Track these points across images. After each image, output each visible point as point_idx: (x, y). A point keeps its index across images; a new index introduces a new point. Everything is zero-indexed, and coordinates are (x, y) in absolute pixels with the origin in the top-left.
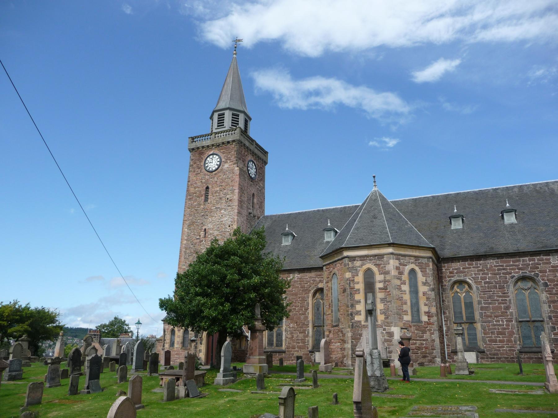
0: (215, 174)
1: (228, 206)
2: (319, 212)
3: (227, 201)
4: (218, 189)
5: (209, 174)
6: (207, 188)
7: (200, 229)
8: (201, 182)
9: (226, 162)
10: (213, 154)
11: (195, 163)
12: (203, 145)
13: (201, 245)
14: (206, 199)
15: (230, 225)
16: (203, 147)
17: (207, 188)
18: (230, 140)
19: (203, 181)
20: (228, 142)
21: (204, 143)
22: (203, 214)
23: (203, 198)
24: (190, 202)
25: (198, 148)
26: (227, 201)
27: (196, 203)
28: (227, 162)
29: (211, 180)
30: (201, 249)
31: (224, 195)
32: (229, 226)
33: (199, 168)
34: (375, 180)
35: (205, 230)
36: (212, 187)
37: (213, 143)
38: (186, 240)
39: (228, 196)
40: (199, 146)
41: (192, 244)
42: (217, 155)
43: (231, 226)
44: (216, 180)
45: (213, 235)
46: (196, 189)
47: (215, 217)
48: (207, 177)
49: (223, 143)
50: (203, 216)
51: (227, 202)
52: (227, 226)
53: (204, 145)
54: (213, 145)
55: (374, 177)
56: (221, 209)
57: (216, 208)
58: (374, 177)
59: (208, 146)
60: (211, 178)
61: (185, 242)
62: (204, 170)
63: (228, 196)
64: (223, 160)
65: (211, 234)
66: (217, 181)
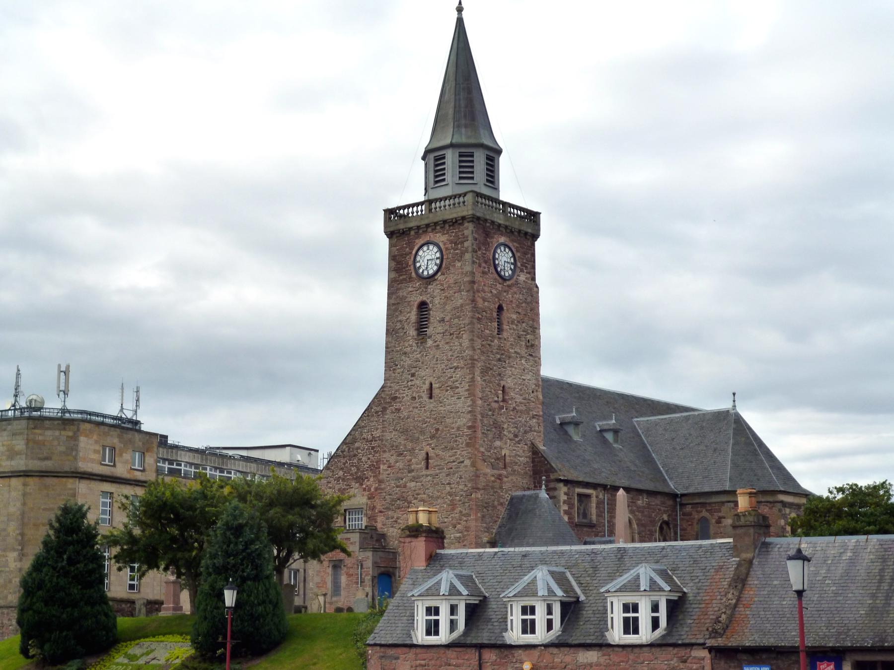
0: (508, 286)
1: (531, 355)
2: (562, 388)
3: (528, 344)
4: (514, 316)
5: (500, 281)
6: (500, 309)
7: (498, 385)
8: (491, 292)
9: (522, 271)
10: (506, 246)
11: (480, 249)
12: (493, 219)
13: (501, 415)
14: (500, 330)
15: (535, 391)
16: (493, 222)
17: (500, 309)
18: (530, 231)
19: (494, 292)
20: (526, 233)
21: (495, 215)
22: (499, 356)
23: (496, 324)
24: (479, 326)
25: (486, 220)
26: (528, 344)
27: (487, 332)
28: (524, 272)
29: (505, 294)
30: (502, 422)
31: (523, 331)
32: (533, 392)
33: (486, 262)
34: (734, 398)
35: (504, 387)
36: (507, 310)
37: (507, 223)
38: (480, 398)
39: (528, 337)
40: (488, 217)
41: (490, 410)
42: (510, 249)
43: (535, 393)
44: (511, 299)
45: (516, 402)
46: (486, 304)
47: (516, 368)
48: (499, 287)
49: (519, 231)
50: (499, 360)
51: (527, 347)
52: (531, 392)
53: (495, 220)
54: (506, 227)
55: (734, 394)
56: (522, 357)
57: (515, 352)
58: (734, 394)
59: (499, 225)
60: (505, 292)
61: (479, 402)
62: (492, 269)
63: (528, 337)
64: (519, 264)
65: (512, 398)
66: (512, 301)
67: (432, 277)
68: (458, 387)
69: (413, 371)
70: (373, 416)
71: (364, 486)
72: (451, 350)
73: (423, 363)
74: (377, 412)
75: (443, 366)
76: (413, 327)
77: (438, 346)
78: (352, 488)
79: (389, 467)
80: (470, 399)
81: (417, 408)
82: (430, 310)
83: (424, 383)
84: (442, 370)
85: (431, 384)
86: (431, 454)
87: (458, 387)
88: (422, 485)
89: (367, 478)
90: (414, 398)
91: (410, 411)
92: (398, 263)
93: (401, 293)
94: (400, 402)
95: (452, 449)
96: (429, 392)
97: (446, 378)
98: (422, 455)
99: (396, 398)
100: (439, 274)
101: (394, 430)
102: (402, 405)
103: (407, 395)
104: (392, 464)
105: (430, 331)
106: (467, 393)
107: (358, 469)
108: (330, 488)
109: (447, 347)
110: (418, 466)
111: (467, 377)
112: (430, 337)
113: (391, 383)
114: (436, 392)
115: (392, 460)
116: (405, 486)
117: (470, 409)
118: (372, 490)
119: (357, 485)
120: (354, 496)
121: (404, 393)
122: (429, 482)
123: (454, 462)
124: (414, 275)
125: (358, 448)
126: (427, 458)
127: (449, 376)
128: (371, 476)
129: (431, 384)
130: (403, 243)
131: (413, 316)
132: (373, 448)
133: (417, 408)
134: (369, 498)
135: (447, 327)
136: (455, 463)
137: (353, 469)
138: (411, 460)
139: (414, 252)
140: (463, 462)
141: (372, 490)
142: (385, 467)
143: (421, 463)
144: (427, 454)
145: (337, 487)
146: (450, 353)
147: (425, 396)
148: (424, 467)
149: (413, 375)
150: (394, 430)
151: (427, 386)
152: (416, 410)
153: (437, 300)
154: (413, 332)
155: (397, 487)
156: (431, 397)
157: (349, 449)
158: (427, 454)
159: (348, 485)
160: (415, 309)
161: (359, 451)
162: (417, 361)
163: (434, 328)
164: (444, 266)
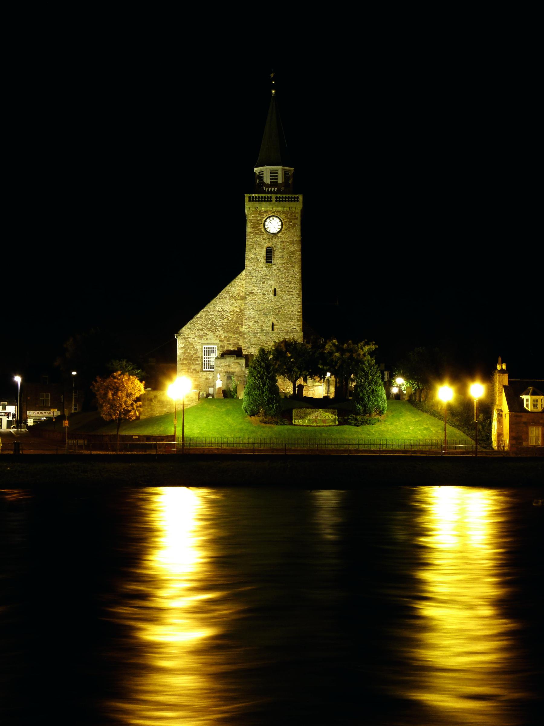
67: (274, 235)
68: (292, 292)
69: (263, 281)
70: (222, 298)
71: (217, 335)
72: (288, 273)
73: (270, 277)
74: (225, 297)
75: (283, 280)
76: (263, 258)
77: (280, 269)
78: (208, 335)
79: (248, 327)
80: (299, 298)
81: (266, 299)
82: (274, 251)
83: (271, 287)
84: (282, 282)
85: (275, 289)
86: (275, 323)
87: (292, 292)
88: (271, 338)
89: (219, 330)
90: (264, 294)
91: (262, 301)
92: (254, 224)
93: (255, 239)
94: (256, 295)
95: (288, 322)
96: (274, 292)
97: (285, 286)
98: (269, 324)
99: (253, 293)
100: (280, 233)
101: (252, 309)
102: (257, 297)
103: (260, 292)
104: (251, 326)
105: (274, 262)
106: (298, 295)
107: (212, 325)
108: (193, 334)
109: (285, 271)
110: (267, 328)
111: (298, 287)
112: (274, 264)
113: (250, 285)
114: (279, 293)
115: (251, 324)
116: (259, 338)
117: (299, 303)
118: (222, 337)
119: (212, 334)
120: (210, 339)
121: (258, 291)
122: (274, 336)
123: (289, 328)
124: (263, 231)
125: (213, 315)
126: (273, 324)
127: (287, 285)
128: (221, 330)
129: (275, 289)
130: (256, 214)
131: (264, 253)
132: (223, 315)
133: (266, 299)
134: (220, 341)
135: (285, 261)
136: (290, 329)
137: (208, 325)
138: (262, 326)
139: (264, 220)
140: (295, 328)
141: (222, 337)
142: (246, 327)
143: (269, 327)
144: (273, 323)
145: (198, 334)
146: (287, 275)
147: (272, 295)
148: (271, 329)
149: (264, 283)
150: (252, 309)
151: (273, 289)
152: (265, 300)
153: (279, 246)
154: (263, 260)
155: (254, 337)
156: (275, 295)
157: (206, 315)
158: (273, 323)
159: (206, 333)
160: (265, 249)
161: (213, 316)
162: (266, 275)
163: (276, 260)
164: (283, 229)
